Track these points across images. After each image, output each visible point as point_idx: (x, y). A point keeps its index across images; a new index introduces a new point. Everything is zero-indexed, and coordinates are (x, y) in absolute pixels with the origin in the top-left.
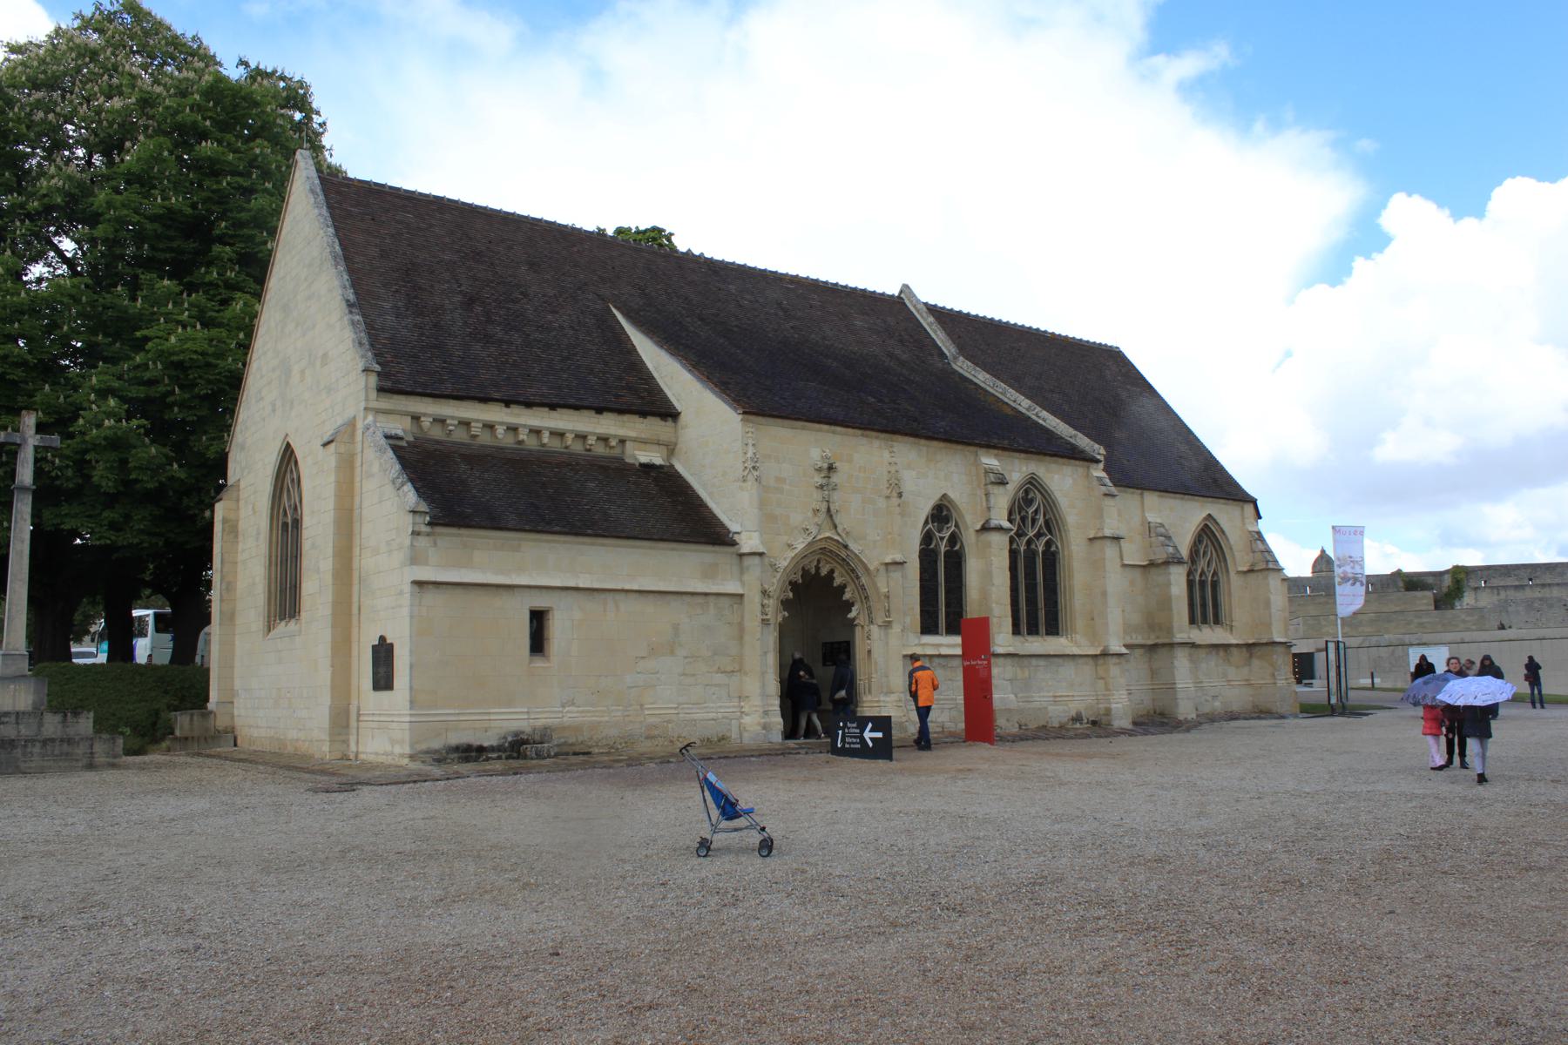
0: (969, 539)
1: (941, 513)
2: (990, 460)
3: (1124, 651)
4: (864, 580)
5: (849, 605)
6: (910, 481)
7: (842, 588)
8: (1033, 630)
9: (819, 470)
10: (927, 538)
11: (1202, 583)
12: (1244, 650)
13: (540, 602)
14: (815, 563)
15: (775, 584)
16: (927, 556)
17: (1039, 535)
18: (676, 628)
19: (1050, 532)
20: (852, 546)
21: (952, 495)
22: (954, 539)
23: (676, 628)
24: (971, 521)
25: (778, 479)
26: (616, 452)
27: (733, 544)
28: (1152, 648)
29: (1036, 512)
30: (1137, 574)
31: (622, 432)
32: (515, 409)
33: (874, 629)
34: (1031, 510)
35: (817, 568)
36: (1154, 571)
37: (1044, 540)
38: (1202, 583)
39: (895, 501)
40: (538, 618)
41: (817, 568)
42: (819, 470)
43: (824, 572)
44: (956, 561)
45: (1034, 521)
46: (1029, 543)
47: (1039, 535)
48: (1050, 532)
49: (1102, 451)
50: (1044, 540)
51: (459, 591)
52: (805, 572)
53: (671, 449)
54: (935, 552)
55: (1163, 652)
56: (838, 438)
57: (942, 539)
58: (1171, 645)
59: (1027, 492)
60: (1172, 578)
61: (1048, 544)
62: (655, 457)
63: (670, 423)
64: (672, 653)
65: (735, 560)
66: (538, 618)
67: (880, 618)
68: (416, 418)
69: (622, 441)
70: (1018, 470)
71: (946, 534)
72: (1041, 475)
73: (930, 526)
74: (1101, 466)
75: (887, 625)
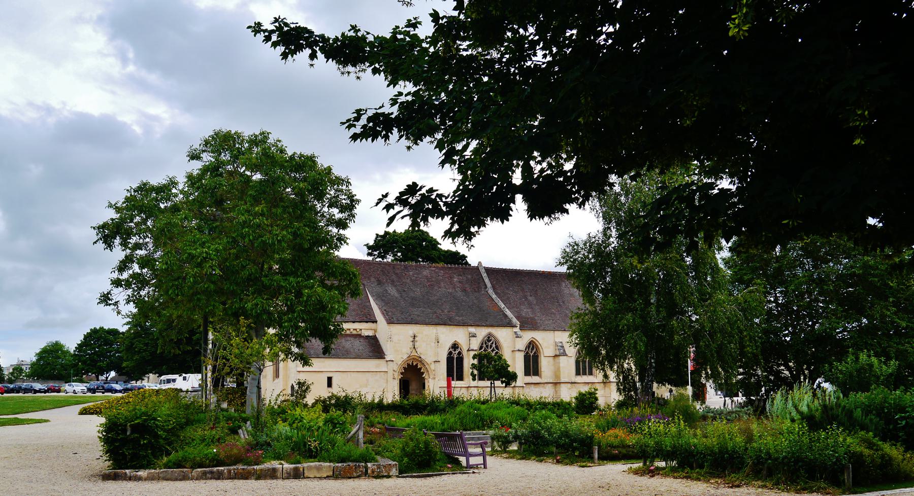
0: (465, 353)
1: (455, 346)
2: (472, 330)
3: (524, 385)
5: (423, 373)
6: (442, 338)
8: (584, 374)
10: (450, 353)
12: (602, 384)
13: (330, 375)
16: (450, 359)
17: (493, 351)
18: (367, 380)
19: (498, 349)
22: (460, 353)
23: (367, 380)
24: (464, 348)
26: (360, 333)
27: (385, 358)
28: (555, 384)
29: (492, 343)
30: (552, 358)
31: (361, 328)
33: (430, 380)
34: (490, 343)
35: (412, 363)
36: (557, 358)
40: (330, 380)
41: (412, 363)
43: (414, 364)
44: (460, 360)
45: (491, 346)
47: (493, 351)
48: (498, 349)
49: (519, 323)
52: (408, 365)
53: (375, 331)
54: (453, 358)
55: (558, 385)
56: (418, 328)
58: (560, 383)
59: (489, 337)
60: (561, 361)
62: (370, 333)
63: (375, 324)
64: (367, 387)
65: (385, 362)
66: (330, 380)
67: (431, 377)
69: (361, 330)
70: (482, 333)
71: (457, 352)
74: (518, 328)
75: (434, 378)
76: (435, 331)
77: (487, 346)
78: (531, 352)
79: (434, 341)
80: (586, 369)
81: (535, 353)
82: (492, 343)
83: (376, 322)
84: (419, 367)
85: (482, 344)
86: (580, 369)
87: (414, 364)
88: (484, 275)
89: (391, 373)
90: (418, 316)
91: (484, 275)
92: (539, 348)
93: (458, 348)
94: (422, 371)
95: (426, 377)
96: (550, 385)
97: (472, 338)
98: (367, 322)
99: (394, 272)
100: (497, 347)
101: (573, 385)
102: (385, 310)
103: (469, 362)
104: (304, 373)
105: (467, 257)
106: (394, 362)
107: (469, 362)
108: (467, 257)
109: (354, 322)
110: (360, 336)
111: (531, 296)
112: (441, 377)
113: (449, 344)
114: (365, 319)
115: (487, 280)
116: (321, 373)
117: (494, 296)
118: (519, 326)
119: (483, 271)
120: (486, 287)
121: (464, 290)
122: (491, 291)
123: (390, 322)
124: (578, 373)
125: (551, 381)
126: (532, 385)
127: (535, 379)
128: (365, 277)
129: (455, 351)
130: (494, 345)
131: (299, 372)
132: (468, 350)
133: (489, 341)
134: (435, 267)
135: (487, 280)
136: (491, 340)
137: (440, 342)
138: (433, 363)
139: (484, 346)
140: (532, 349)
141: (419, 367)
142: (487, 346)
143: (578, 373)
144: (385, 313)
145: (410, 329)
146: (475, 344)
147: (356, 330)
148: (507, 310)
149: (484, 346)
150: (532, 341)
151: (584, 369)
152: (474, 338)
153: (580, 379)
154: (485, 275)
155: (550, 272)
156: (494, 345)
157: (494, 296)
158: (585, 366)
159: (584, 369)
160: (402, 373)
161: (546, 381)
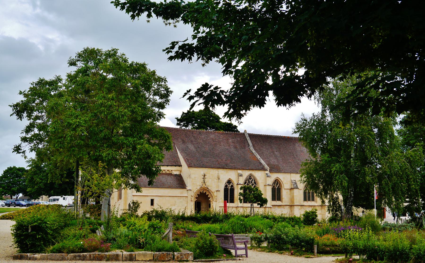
0: (235, 186)
1: (229, 182)
2: (240, 172)
3: (272, 207)
4: (212, 194)
5: (209, 198)
6: (221, 177)
7: (208, 195)
8: (309, 200)
9: (203, 175)
10: (226, 186)
12: (320, 207)
13: (152, 198)
15: (193, 194)
16: (226, 190)
17: (253, 185)
18: (175, 202)
19: (256, 184)
20: (209, 188)
21: (231, 178)
22: (232, 186)
23: (175, 202)
24: (235, 182)
25: (195, 177)
26: (171, 172)
27: (186, 188)
28: (291, 206)
29: (252, 180)
30: (289, 190)
31: (172, 169)
33: (214, 202)
34: (251, 180)
35: (203, 192)
36: (292, 190)
37: (254, 186)
39: (218, 180)
40: (152, 201)
41: (203, 192)
42: (203, 175)
43: (204, 192)
44: (232, 190)
45: (251, 182)
47: (253, 185)
48: (256, 184)
49: (269, 168)
50: (254, 186)
51: (139, 197)
52: (200, 193)
53: (181, 171)
54: (228, 189)
55: (293, 207)
58: (294, 205)
59: (250, 177)
60: (295, 192)
62: (177, 173)
63: (180, 167)
64: (175, 206)
65: (186, 191)
66: (152, 201)
67: (214, 200)
69: (172, 171)
70: (246, 174)
71: (230, 185)
74: (268, 171)
75: (216, 201)
76: (217, 172)
77: (249, 182)
78: (276, 186)
79: (216, 178)
80: (310, 197)
81: (278, 187)
82: (252, 180)
83: (181, 166)
84: (207, 194)
85: (246, 181)
86: (306, 197)
87: (204, 192)
88: (248, 138)
89: (189, 197)
90: (207, 162)
91: (248, 138)
92: (281, 184)
93: (231, 183)
94: (209, 196)
95: (211, 200)
96: (287, 207)
97: (240, 177)
98: (176, 166)
99: (193, 135)
100: (255, 183)
101: (302, 207)
102: (187, 159)
103: (238, 191)
104: (137, 196)
105: (237, 127)
106: (192, 191)
107: (238, 191)
109: (167, 166)
110: (171, 174)
111: (277, 151)
112: (221, 200)
113: (226, 180)
114: (175, 164)
115: (249, 142)
116: (147, 197)
117: (254, 151)
118: (269, 170)
119: (247, 136)
120: (249, 145)
121: (235, 147)
122: (252, 148)
123: (190, 166)
124: (305, 200)
125: (288, 204)
126: (277, 207)
127: (278, 203)
128: (175, 139)
129: (229, 184)
130: (253, 182)
131: (134, 196)
132: (237, 184)
133: (250, 179)
134: (218, 133)
135: (249, 142)
136: (251, 178)
137: (220, 179)
138: (215, 192)
139: (247, 182)
140: (277, 184)
141: (207, 194)
142: (249, 182)
143: (305, 200)
144: (186, 161)
145: (202, 171)
146: (242, 181)
147: (169, 170)
148: (262, 160)
149: (247, 182)
150: (277, 179)
151: (309, 197)
153: (306, 203)
154: (249, 138)
155: (288, 137)
156: (253, 182)
157: (254, 151)
158: (310, 196)
159: (309, 197)
160: (196, 198)
161: (285, 204)
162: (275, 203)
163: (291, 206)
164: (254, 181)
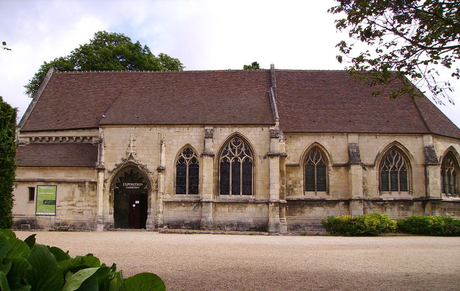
1: (188, 150)
10: (182, 160)
11: (394, 173)
14: (130, 171)
17: (242, 156)
22: (194, 160)
32: (58, 133)
38: (394, 173)
44: (195, 169)
46: (236, 159)
57: (188, 160)
58: (351, 200)
61: (247, 159)
68: (31, 138)
72: (241, 133)
73: (182, 155)
78: (316, 161)
82: (241, 147)
103: (208, 172)
105: (255, 65)
107: (208, 172)
108: (255, 65)
127: (321, 195)
140: (318, 157)
146: (213, 146)
152: (211, 140)
153: (386, 196)
156: (243, 149)
162: (310, 195)
163: (347, 202)
164: (246, 148)
